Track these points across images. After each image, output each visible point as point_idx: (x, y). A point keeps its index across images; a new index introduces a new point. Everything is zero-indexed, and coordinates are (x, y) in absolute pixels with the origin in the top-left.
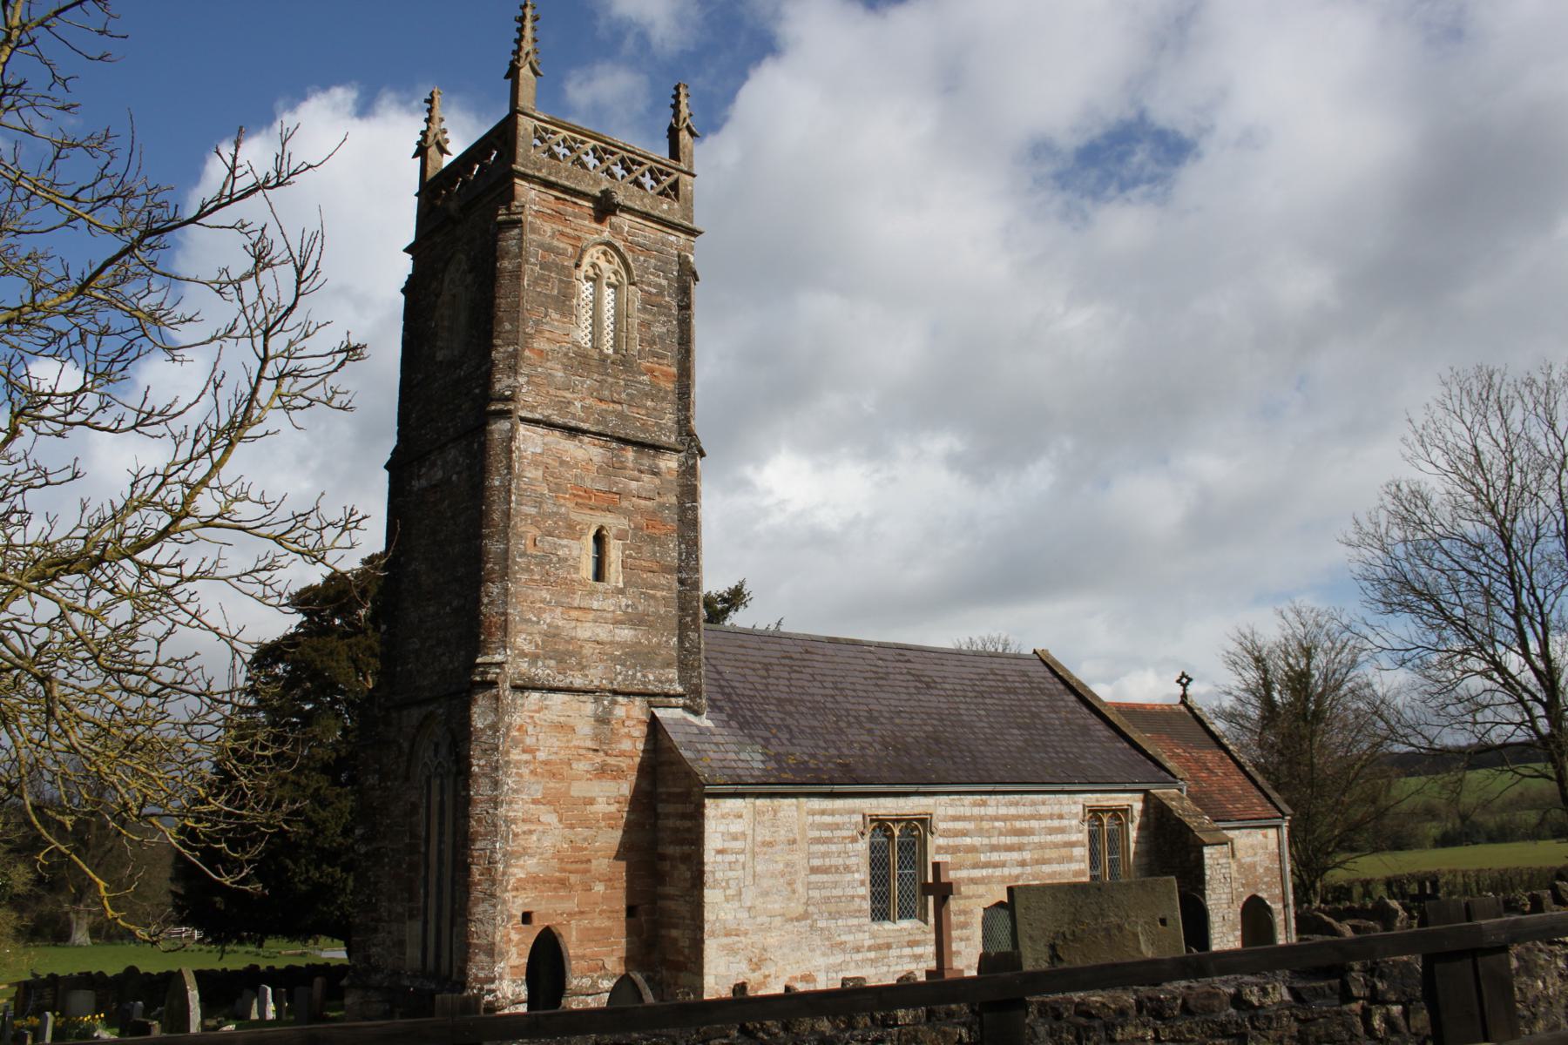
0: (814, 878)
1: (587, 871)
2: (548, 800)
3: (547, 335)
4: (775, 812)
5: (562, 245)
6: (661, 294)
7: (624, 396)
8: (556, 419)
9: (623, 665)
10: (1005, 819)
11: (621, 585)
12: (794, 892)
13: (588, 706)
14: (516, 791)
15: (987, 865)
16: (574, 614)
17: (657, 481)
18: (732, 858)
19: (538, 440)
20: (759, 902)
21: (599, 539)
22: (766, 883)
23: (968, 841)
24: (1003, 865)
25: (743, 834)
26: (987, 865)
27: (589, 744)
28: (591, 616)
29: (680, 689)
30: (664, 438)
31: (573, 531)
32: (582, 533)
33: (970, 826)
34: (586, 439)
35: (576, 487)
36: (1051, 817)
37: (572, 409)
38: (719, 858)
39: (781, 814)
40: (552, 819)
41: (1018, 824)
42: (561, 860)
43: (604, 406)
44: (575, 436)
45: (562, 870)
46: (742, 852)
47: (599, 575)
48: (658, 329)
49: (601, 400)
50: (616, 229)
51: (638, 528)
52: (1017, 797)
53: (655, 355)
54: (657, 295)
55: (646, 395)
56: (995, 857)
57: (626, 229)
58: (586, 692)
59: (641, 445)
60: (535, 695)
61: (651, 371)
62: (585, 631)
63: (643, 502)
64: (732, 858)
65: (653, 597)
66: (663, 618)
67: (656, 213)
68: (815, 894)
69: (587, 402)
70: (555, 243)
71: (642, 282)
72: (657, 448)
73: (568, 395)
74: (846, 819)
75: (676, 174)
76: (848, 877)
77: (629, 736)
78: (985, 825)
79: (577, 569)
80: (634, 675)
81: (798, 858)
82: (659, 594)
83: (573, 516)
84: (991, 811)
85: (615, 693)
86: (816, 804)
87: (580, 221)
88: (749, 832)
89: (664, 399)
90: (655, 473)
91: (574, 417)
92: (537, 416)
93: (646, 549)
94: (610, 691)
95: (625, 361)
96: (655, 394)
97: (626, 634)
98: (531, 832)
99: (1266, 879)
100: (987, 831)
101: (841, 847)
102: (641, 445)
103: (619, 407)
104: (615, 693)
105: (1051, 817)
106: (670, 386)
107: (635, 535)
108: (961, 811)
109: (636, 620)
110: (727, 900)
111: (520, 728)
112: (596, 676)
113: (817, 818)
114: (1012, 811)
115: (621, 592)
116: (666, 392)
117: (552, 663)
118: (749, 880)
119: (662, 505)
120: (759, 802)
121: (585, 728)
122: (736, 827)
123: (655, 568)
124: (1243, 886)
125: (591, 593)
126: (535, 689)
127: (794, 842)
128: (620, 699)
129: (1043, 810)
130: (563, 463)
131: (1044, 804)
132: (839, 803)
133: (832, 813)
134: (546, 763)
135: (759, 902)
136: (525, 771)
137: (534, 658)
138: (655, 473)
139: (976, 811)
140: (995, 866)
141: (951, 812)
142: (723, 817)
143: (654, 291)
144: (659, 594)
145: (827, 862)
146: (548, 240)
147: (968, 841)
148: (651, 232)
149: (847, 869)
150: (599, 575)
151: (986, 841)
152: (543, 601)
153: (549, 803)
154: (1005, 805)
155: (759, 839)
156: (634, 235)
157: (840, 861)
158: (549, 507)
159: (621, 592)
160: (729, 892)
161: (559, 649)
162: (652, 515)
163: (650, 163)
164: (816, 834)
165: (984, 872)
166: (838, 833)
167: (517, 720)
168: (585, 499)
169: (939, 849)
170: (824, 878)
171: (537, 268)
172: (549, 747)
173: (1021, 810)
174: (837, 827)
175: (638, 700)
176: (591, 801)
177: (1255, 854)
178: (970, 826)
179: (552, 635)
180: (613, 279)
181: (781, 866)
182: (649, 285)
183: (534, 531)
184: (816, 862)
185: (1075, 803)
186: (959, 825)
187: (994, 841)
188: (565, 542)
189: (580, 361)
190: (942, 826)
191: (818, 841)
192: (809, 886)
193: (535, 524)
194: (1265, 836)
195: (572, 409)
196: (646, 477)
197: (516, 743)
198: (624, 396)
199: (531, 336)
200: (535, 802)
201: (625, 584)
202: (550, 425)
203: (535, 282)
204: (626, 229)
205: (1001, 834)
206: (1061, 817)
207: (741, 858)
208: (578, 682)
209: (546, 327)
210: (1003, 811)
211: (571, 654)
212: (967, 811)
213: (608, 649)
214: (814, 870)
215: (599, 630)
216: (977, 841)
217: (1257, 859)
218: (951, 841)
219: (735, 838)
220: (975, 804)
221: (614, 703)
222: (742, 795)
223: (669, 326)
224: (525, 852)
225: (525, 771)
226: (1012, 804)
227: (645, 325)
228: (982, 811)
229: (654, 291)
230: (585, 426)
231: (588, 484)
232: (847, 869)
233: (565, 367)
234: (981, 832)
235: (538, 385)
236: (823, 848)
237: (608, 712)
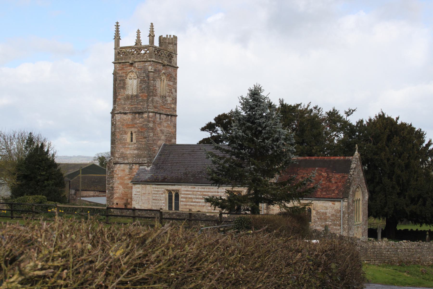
0: (153, 201)
1: (127, 197)
2: (121, 184)
3: (121, 95)
4: (146, 187)
5: (123, 75)
6: (144, 78)
7: (136, 103)
8: (122, 112)
9: (135, 158)
10: (201, 192)
11: (135, 142)
12: (149, 203)
13: (128, 166)
14: (115, 182)
15: (195, 202)
16: (126, 149)
17: (143, 119)
18: (137, 196)
19: (119, 116)
20: (142, 205)
21: (132, 134)
22: (144, 201)
23: (190, 196)
24: (200, 202)
25: (140, 192)
26: (195, 202)
27: (128, 173)
28: (129, 149)
29: (146, 162)
30: (144, 110)
31: (126, 133)
32: (128, 133)
33: (191, 193)
34: (128, 114)
35: (127, 124)
36: (215, 192)
37: (126, 109)
38: (135, 196)
39: (147, 188)
40: (121, 187)
41: (204, 193)
42: (123, 194)
43: (132, 106)
44: (126, 114)
45: (123, 196)
46: (139, 195)
47: (132, 141)
48: (143, 86)
49: (131, 105)
50: (135, 67)
51: (139, 130)
52: (204, 187)
53: (142, 92)
54: (143, 78)
55: (141, 102)
56: (197, 200)
57: (137, 66)
58: (127, 164)
59: (139, 113)
60: (118, 165)
61: (142, 96)
62: (128, 152)
63: (140, 125)
64: (137, 196)
65: (142, 144)
66: (143, 148)
67: (143, 60)
68: (153, 204)
69: (129, 107)
70: (122, 75)
71: (140, 77)
72: (142, 113)
73: (125, 106)
74: (161, 189)
75: (148, 48)
76: (161, 202)
77: (135, 172)
78: (195, 193)
79: (126, 140)
80: (137, 160)
81: (150, 197)
82: (143, 143)
83: (126, 130)
84: (196, 190)
85: (133, 164)
86: (154, 186)
87: (127, 68)
88: (141, 191)
89: (145, 101)
90: (142, 118)
91: (126, 110)
92: (119, 112)
93: (140, 134)
94: (132, 163)
95: (137, 96)
96: (143, 101)
97: (136, 152)
98: (118, 189)
99: (331, 218)
100: (195, 194)
101: (159, 195)
102: (139, 113)
103: (135, 106)
104: (133, 164)
105: (215, 192)
106: (145, 98)
107: (138, 132)
108: (189, 189)
109: (138, 149)
110: (136, 203)
111: (116, 171)
112: (130, 161)
113: (154, 189)
114: (203, 190)
115: (135, 143)
116: (145, 100)
117: (122, 159)
118: (140, 200)
119: (144, 125)
120: (143, 185)
121: (127, 171)
122: (138, 190)
123: (142, 137)
124: (318, 219)
125: (129, 145)
126: (118, 164)
127: (149, 194)
128: (134, 165)
129: (212, 190)
130: (124, 120)
131: (213, 189)
132: (159, 186)
133: (158, 188)
134: (120, 177)
135: (142, 205)
136: (116, 178)
137: (119, 158)
138: (142, 118)
139: (192, 189)
140: (197, 202)
141: (185, 189)
142: (136, 188)
143: (142, 78)
144: (143, 143)
145: (156, 198)
146: (121, 75)
147: (190, 196)
148: (141, 64)
149: (161, 200)
150: (132, 141)
151: (195, 196)
152: (120, 147)
153: (121, 184)
154: (201, 188)
155: (143, 193)
156: (138, 66)
157: (159, 198)
158: (121, 129)
159: (135, 143)
160: (137, 202)
161: (123, 156)
162: (142, 128)
163: (142, 48)
164: (154, 192)
165: (194, 204)
166: (158, 192)
167: (115, 169)
168: (128, 126)
169: (182, 197)
170: (156, 201)
171: (119, 82)
172: (120, 174)
173: (205, 190)
174: (158, 191)
175: (137, 165)
176: (128, 184)
177: (327, 209)
178: (191, 193)
179: (122, 153)
180: (135, 78)
181: (147, 198)
182: (142, 77)
183: (118, 134)
184: (154, 198)
185: (223, 189)
186: (188, 192)
187: (197, 197)
188: (124, 135)
189: (128, 98)
190: (183, 192)
191: (154, 194)
192: (152, 202)
193: (119, 133)
194: (334, 204)
195: (126, 109)
196: (140, 119)
197: (115, 173)
198: (136, 103)
199: (118, 96)
200: (118, 184)
201: (136, 142)
202: (121, 113)
203: (118, 85)
204: (137, 66)
205: (199, 195)
206: (218, 192)
207: (139, 196)
208: (126, 161)
209: (121, 93)
210: (200, 190)
211: (126, 157)
212: (190, 189)
213: (132, 155)
214: (154, 199)
215: (131, 152)
216: (192, 196)
217: (328, 211)
218: (185, 196)
219: (138, 192)
220: (192, 188)
221: (133, 165)
222: (140, 184)
223: (146, 85)
224: (116, 193)
225: (116, 178)
226: (203, 188)
227: (141, 86)
228: (194, 189)
229: (142, 78)
230: (127, 112)
231: (129, 123)
232: (161, 200)
233: (124, 101)
234: (193, 194)
235: (119, 105)
236: (155, 195)
237: (132, 167)
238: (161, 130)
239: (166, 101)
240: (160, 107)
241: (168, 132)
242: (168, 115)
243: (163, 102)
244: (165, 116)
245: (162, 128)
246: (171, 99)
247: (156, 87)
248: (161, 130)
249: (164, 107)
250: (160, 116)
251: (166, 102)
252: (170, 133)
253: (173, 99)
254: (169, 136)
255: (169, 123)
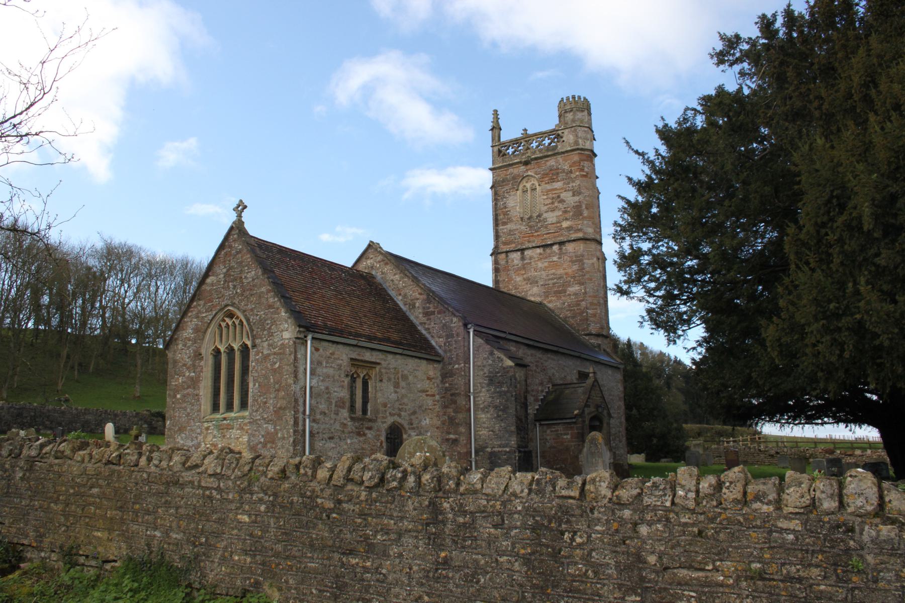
238: (527, 280)
239: (540, 221)
240: (523, 237)
241: (551, 277)
242: (545, 246)
243: (531, 227)
244: (539, 251)
245: (532, 273)
246: (561, 213)
247: (505, 207)
248: (527, 280)
249: (536, 234)
250: (523, 254)
251: (539, 225)
252: (560, 278)
253: (565, 212)
254: (554, 284)
255: (555, 259)
